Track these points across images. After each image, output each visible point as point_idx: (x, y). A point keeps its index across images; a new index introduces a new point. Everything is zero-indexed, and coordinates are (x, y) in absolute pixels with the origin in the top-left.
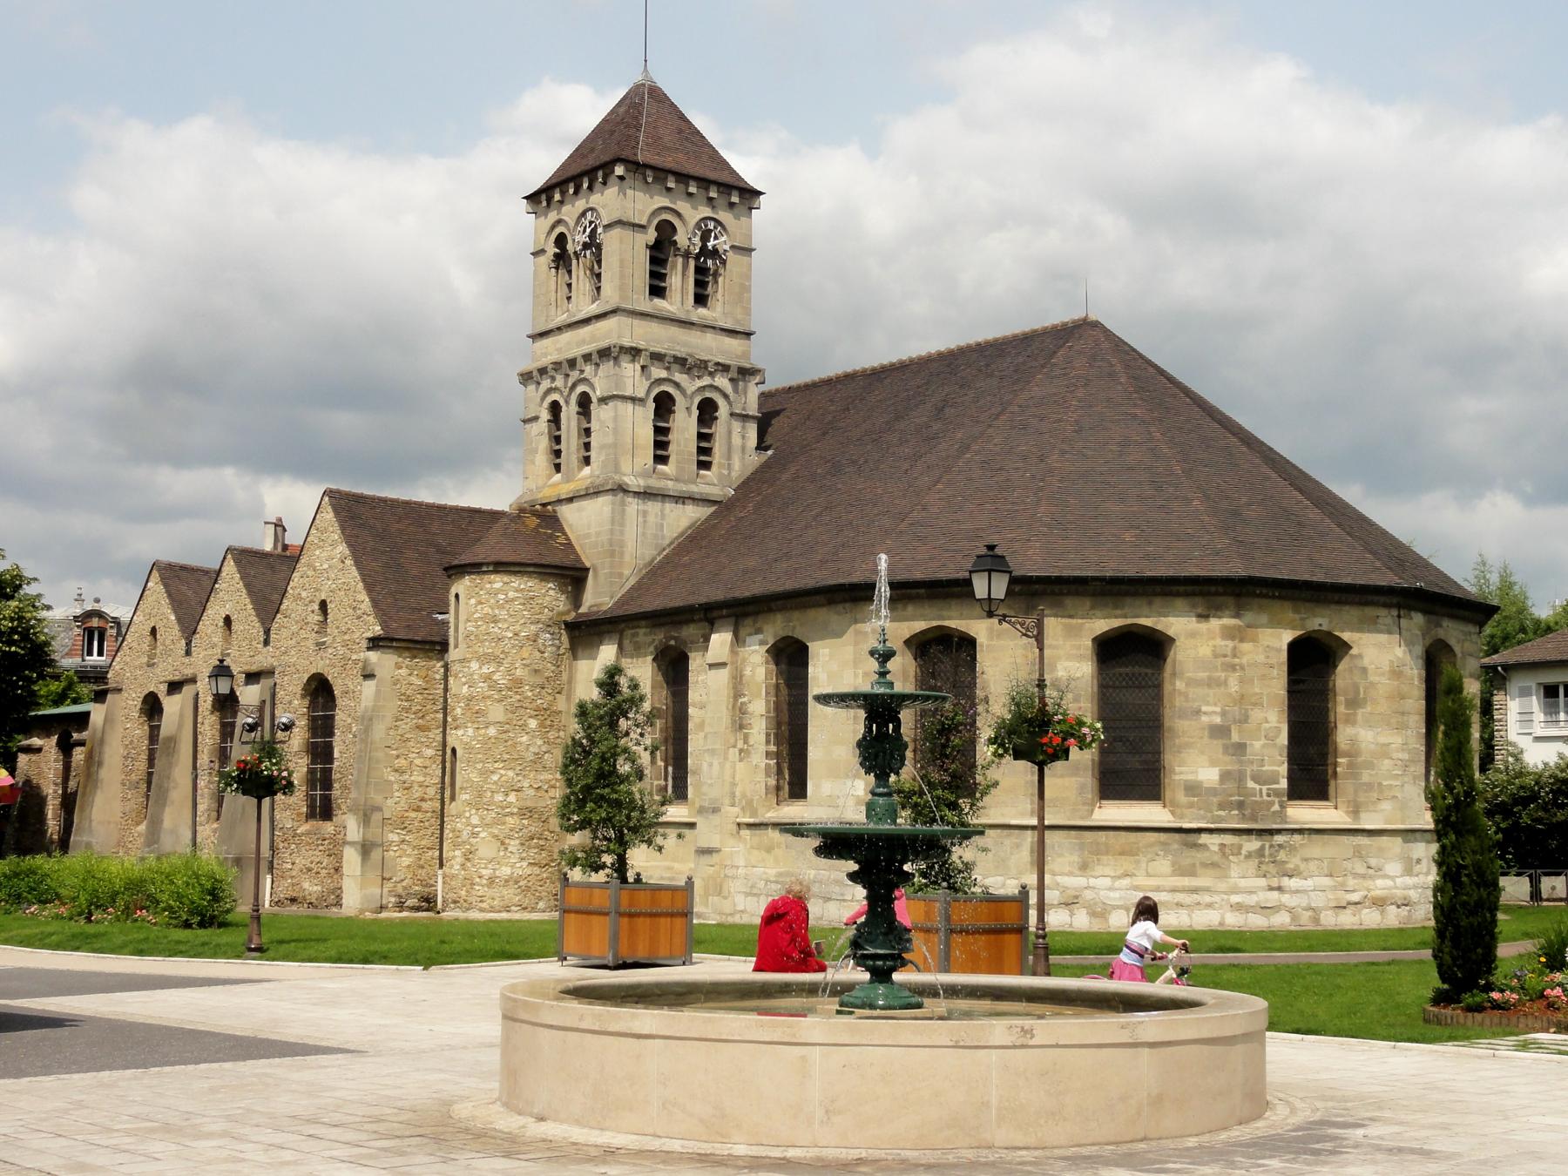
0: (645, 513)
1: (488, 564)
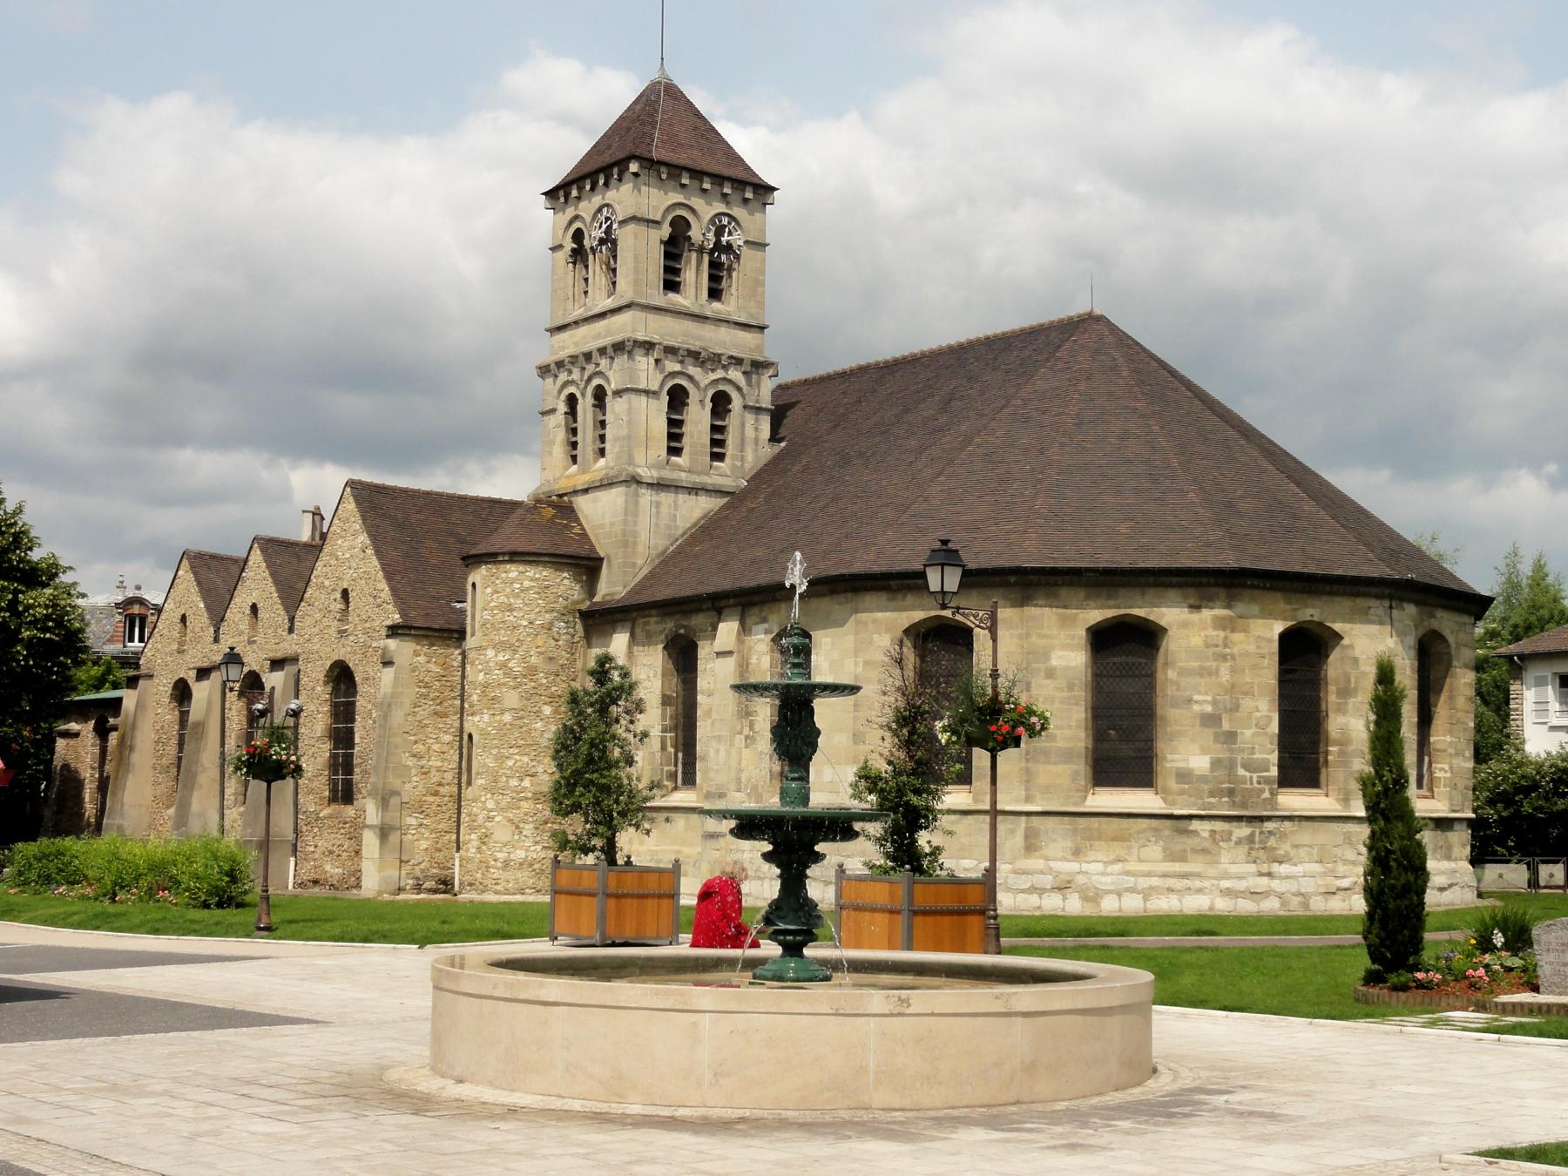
0: (658, 504)
1: (504, 554)
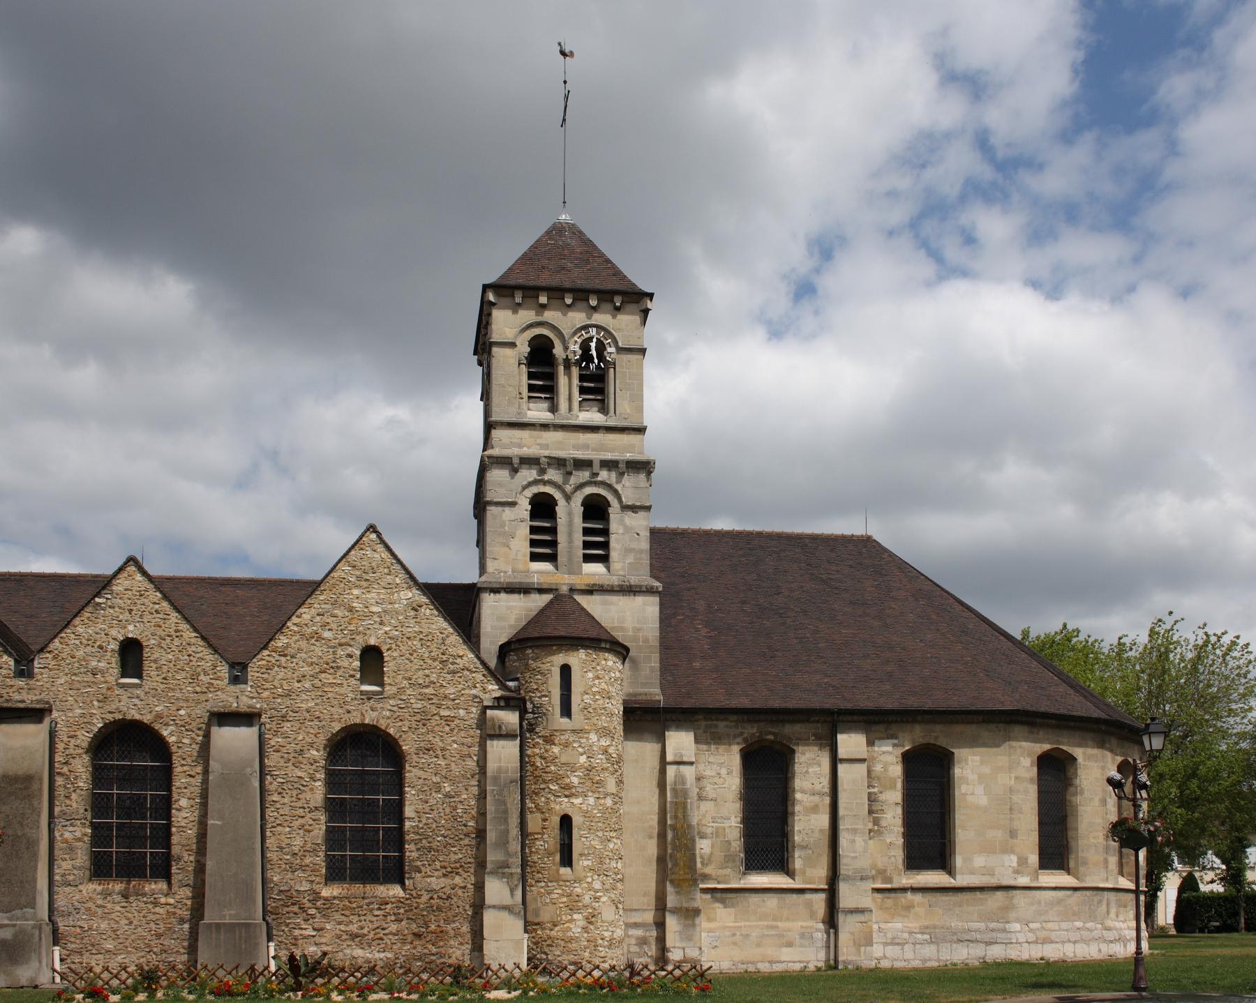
1: (606, 641)
